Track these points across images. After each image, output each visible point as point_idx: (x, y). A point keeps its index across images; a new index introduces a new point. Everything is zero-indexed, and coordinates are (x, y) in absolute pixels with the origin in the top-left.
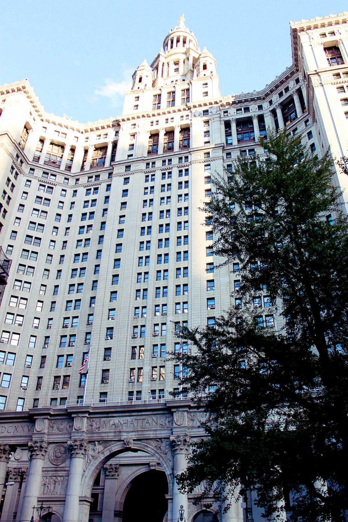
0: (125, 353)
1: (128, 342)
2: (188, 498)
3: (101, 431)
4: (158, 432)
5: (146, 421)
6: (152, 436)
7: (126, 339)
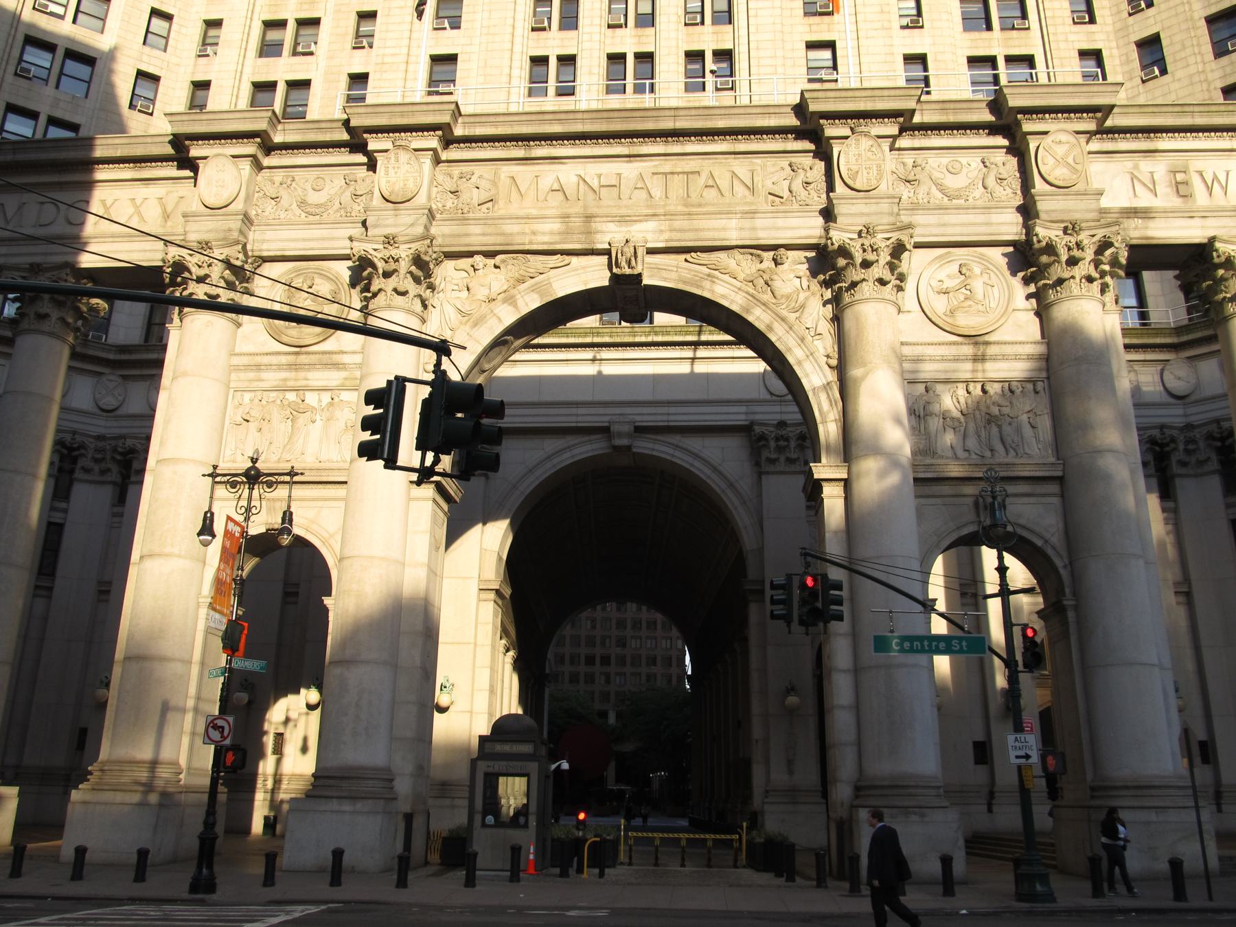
0: (507, 71)
1: (518, 40)
2: (915, 480)
3: (502, 212)
4: (759, 223)
5: (702, 180)
6: (733, 238)
7: (510, 30)
